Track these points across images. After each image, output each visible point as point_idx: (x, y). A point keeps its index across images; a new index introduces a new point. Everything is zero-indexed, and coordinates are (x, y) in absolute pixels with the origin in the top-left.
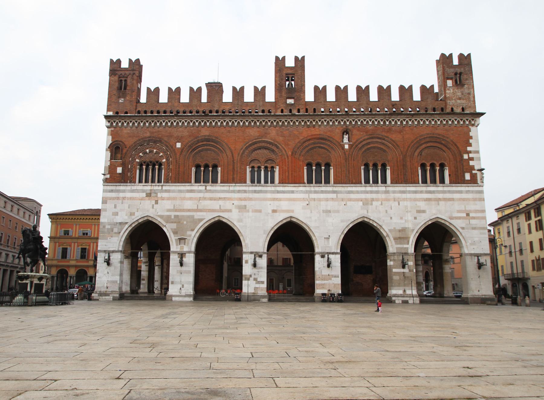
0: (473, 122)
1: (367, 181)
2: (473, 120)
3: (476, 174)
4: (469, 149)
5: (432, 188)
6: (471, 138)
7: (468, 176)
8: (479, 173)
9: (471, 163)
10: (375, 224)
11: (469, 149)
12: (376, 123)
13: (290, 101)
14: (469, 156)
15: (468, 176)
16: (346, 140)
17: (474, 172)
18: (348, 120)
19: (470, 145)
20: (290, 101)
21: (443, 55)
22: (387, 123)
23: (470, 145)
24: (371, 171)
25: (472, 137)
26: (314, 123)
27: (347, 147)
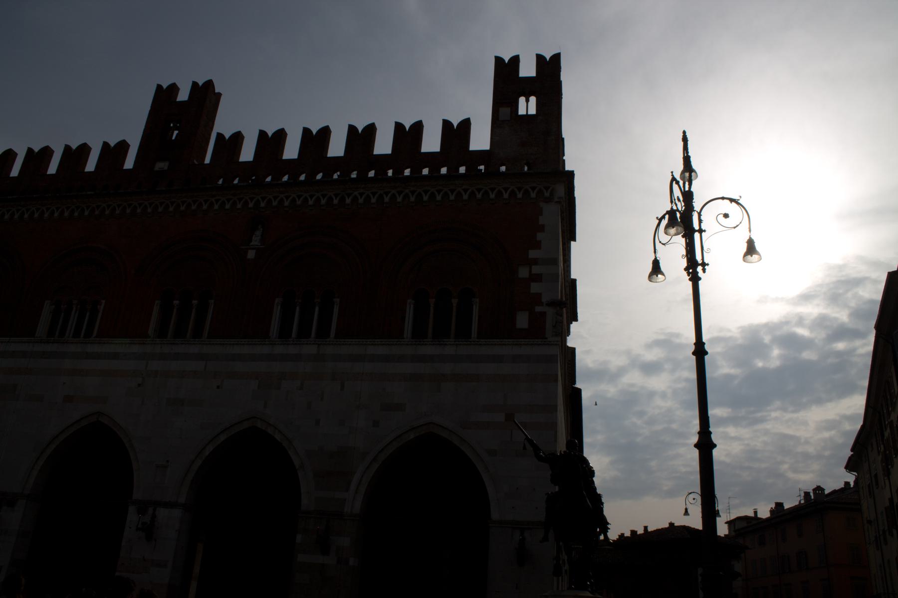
0: (547, 194)
1: (284, 334)
2: (547, 188)
3: (543, 314)
4: (533, 254)
5: (428, 349)
6: (542, 228)
7: (522, 320)
8: (550, 312)
9: (535, 288)
10: (278, 437)
11: (533, 254)
12: (323, 202)
13: (162, 165)
14: (530, 271)
15: (522, 320)
16: (256, 241)
17: (538, 309)
18: (263, 199)
19: (537, 245)
20: (162, 165)
21: (499, 60)
22: (348, 201)
23: (537, 245)
24: (298, 308)
25: (543, 226)
26: (194, 207)
27: (251, 254)
